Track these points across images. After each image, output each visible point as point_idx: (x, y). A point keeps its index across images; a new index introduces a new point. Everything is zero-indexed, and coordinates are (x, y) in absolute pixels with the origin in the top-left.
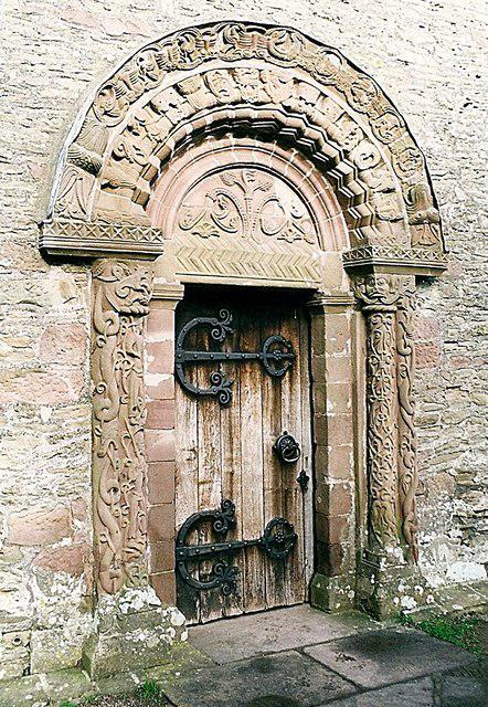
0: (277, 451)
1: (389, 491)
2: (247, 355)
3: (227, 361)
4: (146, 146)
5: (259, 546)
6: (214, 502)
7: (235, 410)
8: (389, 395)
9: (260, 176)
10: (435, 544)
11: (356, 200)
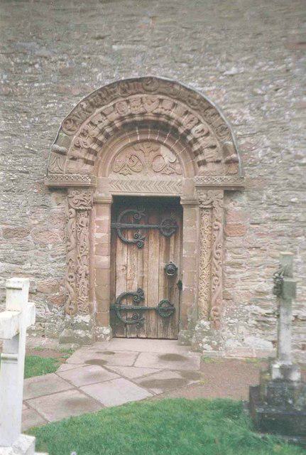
1: (204, 294)
2: (152, 226)
3: (142, 228)
4: (88, 141)
5: (156, 310)
6: (134, 289)
7: (146, 250)
9: (155, 146)
10: (237, 325)
11: (196, 154)
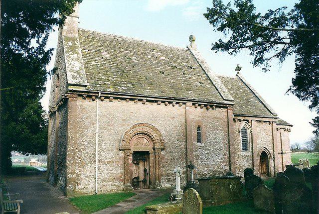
0: (144, 170)
8: (157, 164)
